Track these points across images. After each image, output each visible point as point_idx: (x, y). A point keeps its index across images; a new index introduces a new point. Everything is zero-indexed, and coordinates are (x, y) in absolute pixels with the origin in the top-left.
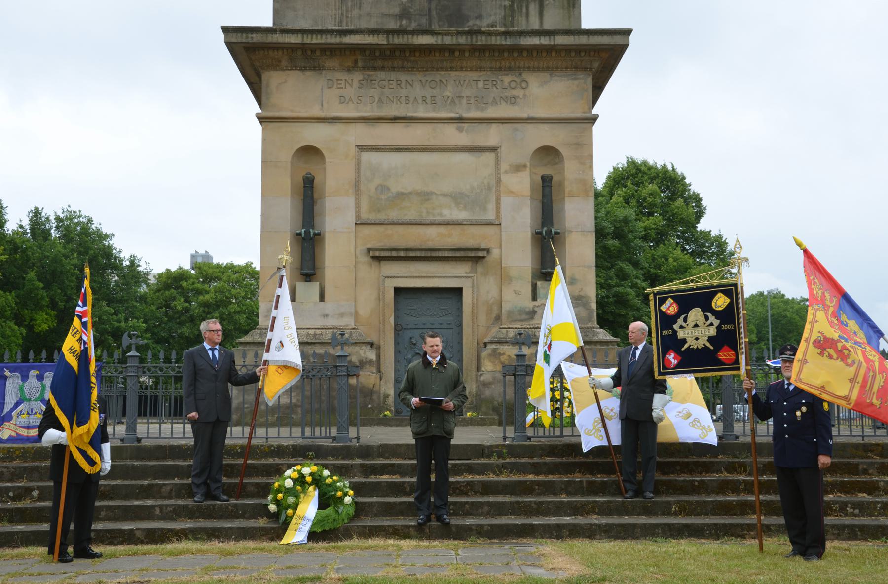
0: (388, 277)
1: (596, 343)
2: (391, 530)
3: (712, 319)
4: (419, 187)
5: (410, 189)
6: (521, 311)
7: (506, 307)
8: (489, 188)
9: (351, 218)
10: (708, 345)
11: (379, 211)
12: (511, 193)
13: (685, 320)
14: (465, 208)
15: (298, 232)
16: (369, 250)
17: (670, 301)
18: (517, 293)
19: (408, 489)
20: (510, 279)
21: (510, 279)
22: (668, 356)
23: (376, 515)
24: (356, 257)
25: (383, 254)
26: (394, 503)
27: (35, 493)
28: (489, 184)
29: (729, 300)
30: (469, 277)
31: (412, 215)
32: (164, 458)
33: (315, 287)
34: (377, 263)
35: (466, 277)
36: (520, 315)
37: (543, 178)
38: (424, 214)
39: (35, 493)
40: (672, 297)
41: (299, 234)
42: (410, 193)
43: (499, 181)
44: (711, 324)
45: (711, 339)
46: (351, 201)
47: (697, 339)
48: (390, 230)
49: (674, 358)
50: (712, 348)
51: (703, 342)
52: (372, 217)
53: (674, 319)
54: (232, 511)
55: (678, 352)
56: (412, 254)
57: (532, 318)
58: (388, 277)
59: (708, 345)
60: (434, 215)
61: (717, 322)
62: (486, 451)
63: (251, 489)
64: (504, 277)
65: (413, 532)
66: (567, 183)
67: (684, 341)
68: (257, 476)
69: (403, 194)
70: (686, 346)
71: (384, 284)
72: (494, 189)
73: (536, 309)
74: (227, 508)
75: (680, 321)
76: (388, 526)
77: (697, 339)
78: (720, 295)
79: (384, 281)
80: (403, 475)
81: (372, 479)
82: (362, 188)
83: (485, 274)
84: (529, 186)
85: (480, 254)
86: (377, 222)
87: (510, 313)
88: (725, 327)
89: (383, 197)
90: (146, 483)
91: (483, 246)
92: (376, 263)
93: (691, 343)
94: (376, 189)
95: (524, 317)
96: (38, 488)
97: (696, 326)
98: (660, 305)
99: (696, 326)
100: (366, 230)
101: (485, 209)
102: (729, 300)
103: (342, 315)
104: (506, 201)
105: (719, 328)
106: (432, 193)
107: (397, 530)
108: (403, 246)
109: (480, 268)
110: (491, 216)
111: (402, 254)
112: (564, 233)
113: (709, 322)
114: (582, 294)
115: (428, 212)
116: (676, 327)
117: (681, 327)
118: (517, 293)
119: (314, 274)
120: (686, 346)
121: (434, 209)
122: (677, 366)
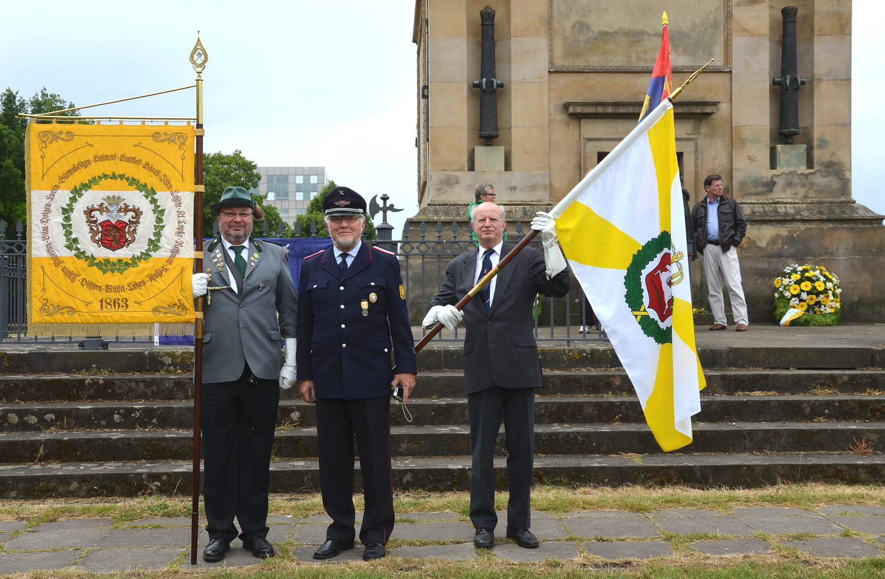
0: (590, 140)
1: (856, 221)
2: (831, 471)
4: (626, 24)
5: (615, 28)
6: (757, 182)
7: (738, 176)
8: (716, 26)
9: (543, 65)
11: (577, 56)
12: (745, 31)
14: (685, 52)
15: (476, 82)
16: (566, 106)
18: (751, 159)
19: (808, 411)
20: (743, 142)
21: (743, 142)
23: (785, 449)
24: (550, 115)
25: (587, 110)
26: (811, 431)
27: (295, 415)
28: (715, 20)
30: (691, 140)
31: (618, 61)
32: (438, 368)
33: (497, 154)
34: (576, 122)
35: (688, 140)
36: (756, 187)
37: (785, 12)
38: (634, 60)
39: (295, 415)
41: (479, 86)
42: (616, 33)
43: (729, 16)
46: (543, 43)
48: (592, 80)
52: (569, 63)
54: (583, 442)
56: (622, 110)
57: (771, 191)
58: (590, 140)
60: (646, 61)
62: (878, 357)
63: (589, 410)
64: (735, 140)
65: (863, 475)
66: (816, 18)
68: (581, 392)
69: (606, 34)
71: (585, 149)
72: (722, 27)
73: (775, 179)
74: (576, 438)
76: (827, 466)
79: (585, 145)
80: (781, 390)
81: (740, 397)
82: (556, 25)
83: (711, 136)
84: (768, 22)
85: (708, 110)
86: (576, 69)
87: (742, 184)
89: (581, 38)
90: (443, 402)
91: (708, 99)
92: (573, 125)
94: (573, 27)
95: (760, 189)
96: (299, 408)
100: (563, 81)
101: (710, 54)
103: (533, 188)
104: (738, 42)
106: (643, 33)
107: (841, 471)
108: (608, 100)
109: (704, 129)
110: (717, 61)
111: (610, 110)
112: (812, 83)
114: (834, 159)
115: (638, 58)
118: (751, 159)
119: (497, 137)
121: (645, 53)
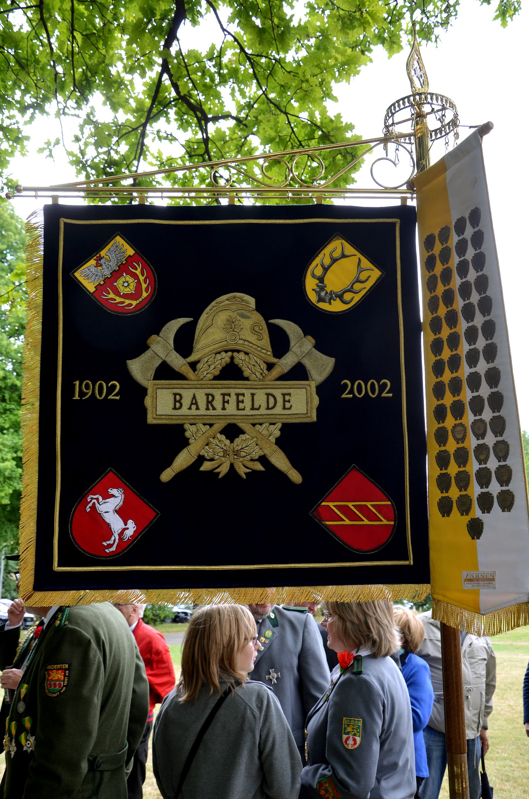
3: (302, 347)
10: (280, 461)
13: (184, 343)
17: (120, 248)
22: (92, 499)
29: (375, 274)
40: (131, 235)
44: (299, 373)
45: (292, 437)
47: (232, 431)
49: (123, 513)
50: (296, 477)
51: (260, 447)
53: (137, 331)
55: (143, 488)
59: (280, 461)
61: (321, 366)
67: (174, 437)
70: (182, 460)
75: (162, 346)
77: (232, 431)
78: (337, 246)
88: (355, 389)
93: (205, 448)
97: (231, 372)
98: (75, 260)
99: (231, 372)
102: (374, 274)
105: (327, 391)
113: (287, 362)
116: (139, 368)
117: (165, 372)
120: (182, 460)
122: (131, 551)
